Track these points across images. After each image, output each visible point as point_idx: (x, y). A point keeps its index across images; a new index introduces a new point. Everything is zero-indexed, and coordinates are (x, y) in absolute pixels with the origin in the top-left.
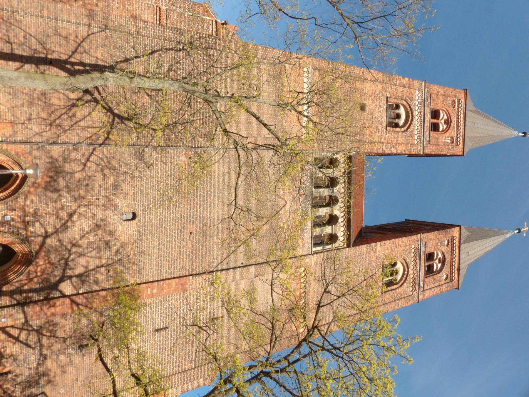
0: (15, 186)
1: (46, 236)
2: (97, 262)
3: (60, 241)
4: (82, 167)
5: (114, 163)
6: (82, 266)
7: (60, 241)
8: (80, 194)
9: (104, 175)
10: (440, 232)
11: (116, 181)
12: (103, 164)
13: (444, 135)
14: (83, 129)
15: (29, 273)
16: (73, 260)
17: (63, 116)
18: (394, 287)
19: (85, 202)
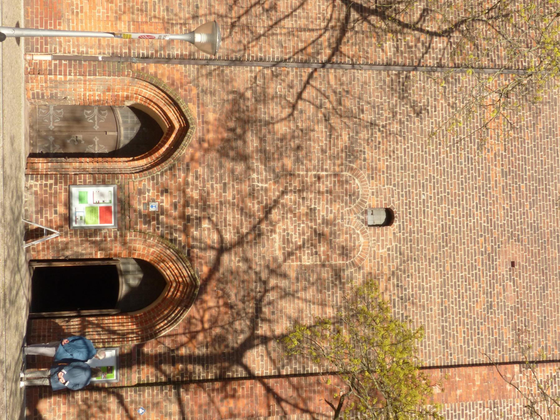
0: (167, 146)
1: (222, 249)
2: (316, 311)
3: (246, 260)
4: (287, 111)
5: (348, 103)
6: (289, 318)
7: (246, 260)
8: (283, 165)
9: (332, 129)
11: (353, 140)
12: (328, 105)
14: (290, 33)
15: (189, 321)
16: (270, 303)
17: (253, 10)
19: (296, 183)
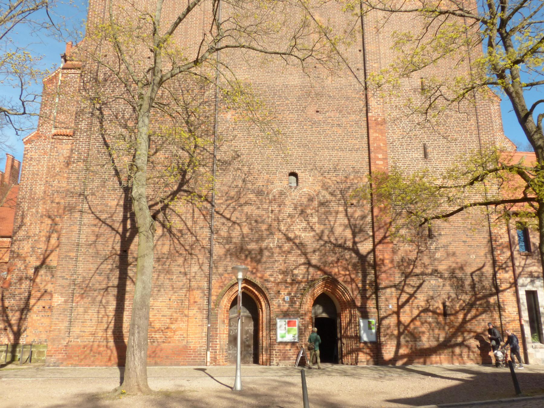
0: (254, 291)
1: (309, 264)
2: (341, 216)
3: (314, 251)
4: (236, 226)
5: (233, 193)
6: (344, 230)
7: (314, 251)
8: (266, 230)
9: (246, 203)
11: (253, 192)
12: (234, 204)
14: (195, 222)
15: (345, 282)
16: (336, 240)
17: (182, 242)
19: (275, 224)
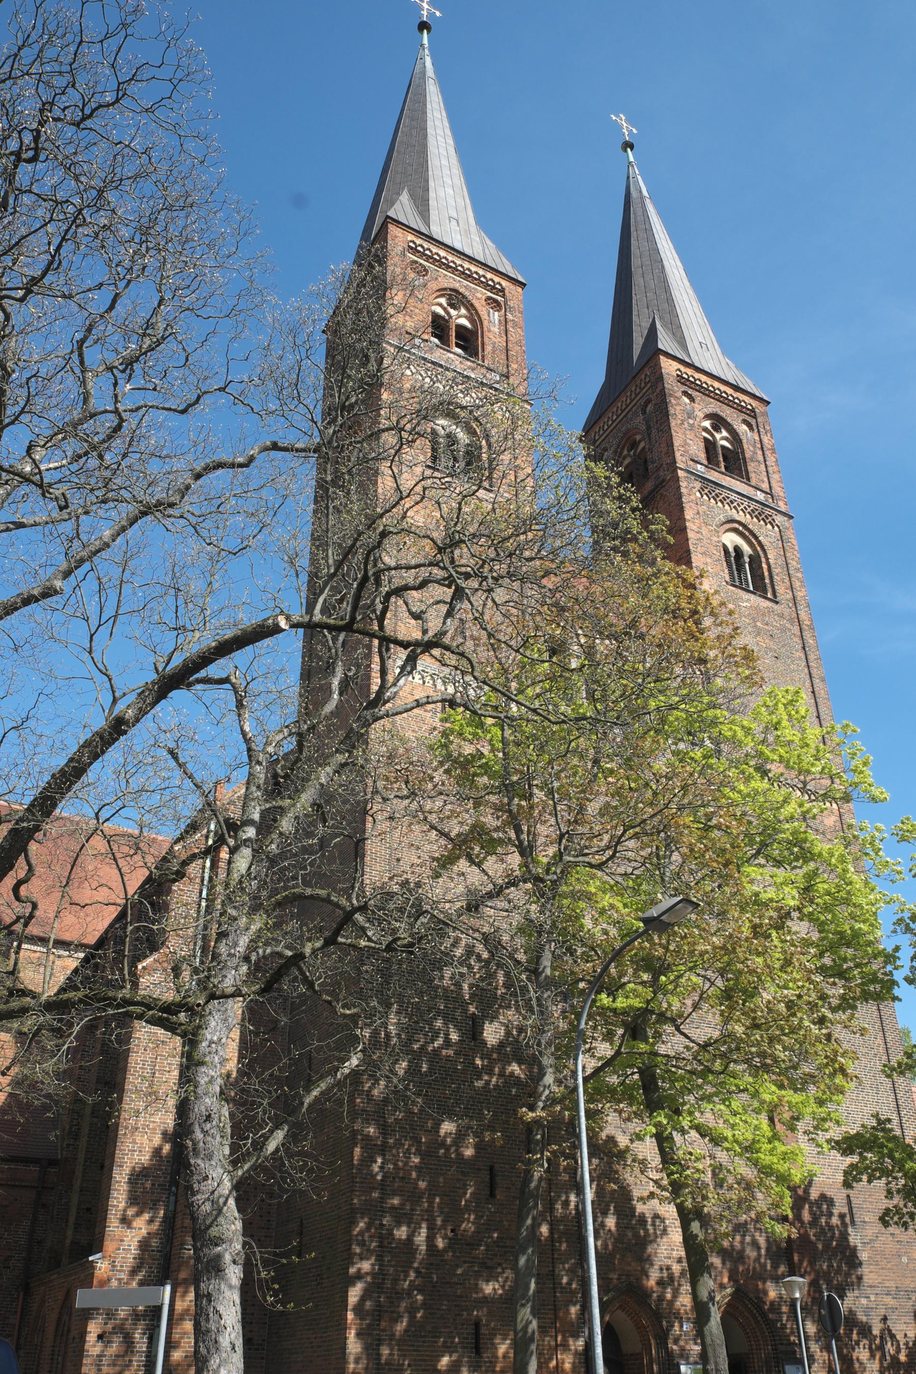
10: (672, 411)
13: (485, 323)
18: (764, 566)
